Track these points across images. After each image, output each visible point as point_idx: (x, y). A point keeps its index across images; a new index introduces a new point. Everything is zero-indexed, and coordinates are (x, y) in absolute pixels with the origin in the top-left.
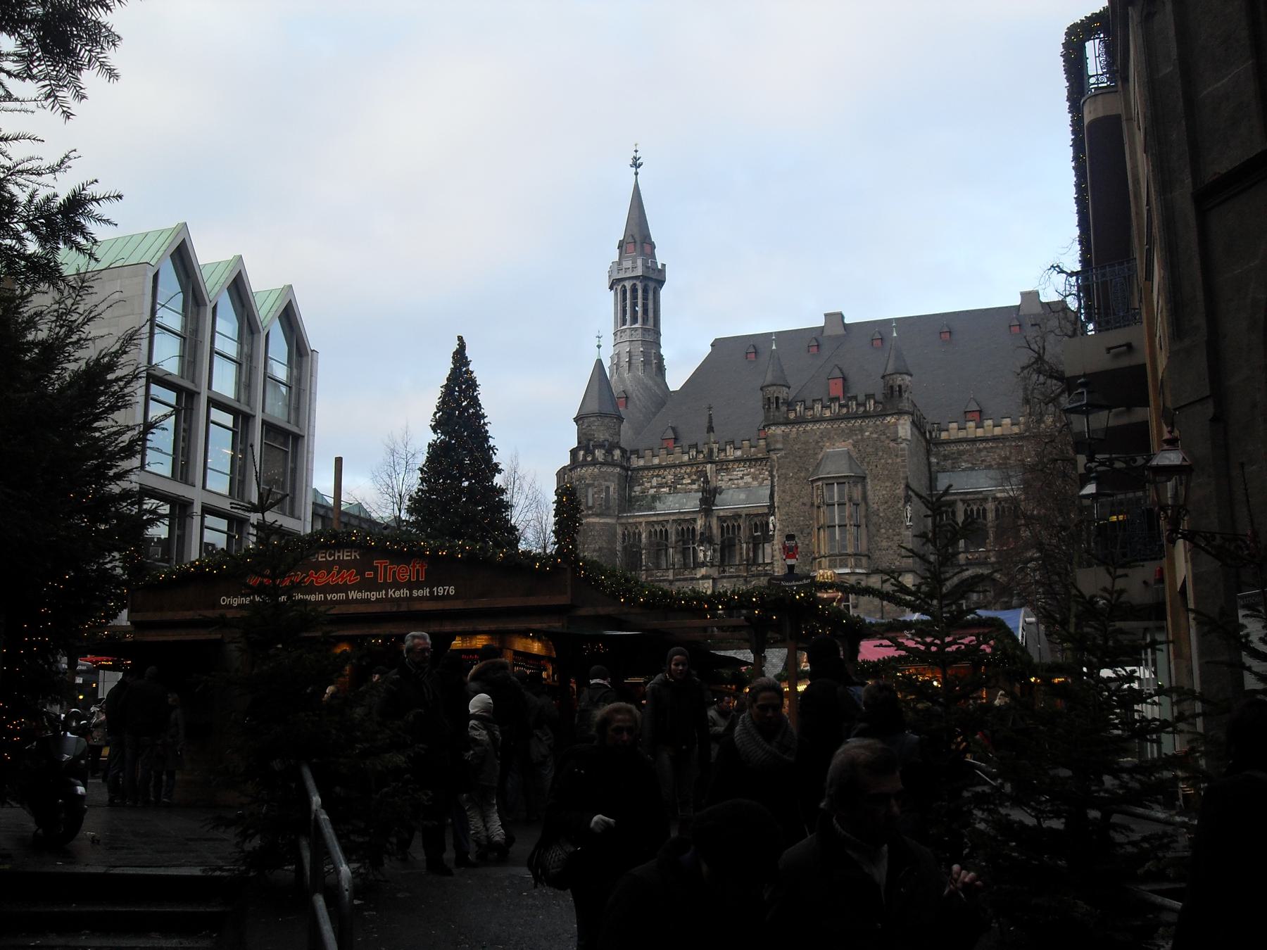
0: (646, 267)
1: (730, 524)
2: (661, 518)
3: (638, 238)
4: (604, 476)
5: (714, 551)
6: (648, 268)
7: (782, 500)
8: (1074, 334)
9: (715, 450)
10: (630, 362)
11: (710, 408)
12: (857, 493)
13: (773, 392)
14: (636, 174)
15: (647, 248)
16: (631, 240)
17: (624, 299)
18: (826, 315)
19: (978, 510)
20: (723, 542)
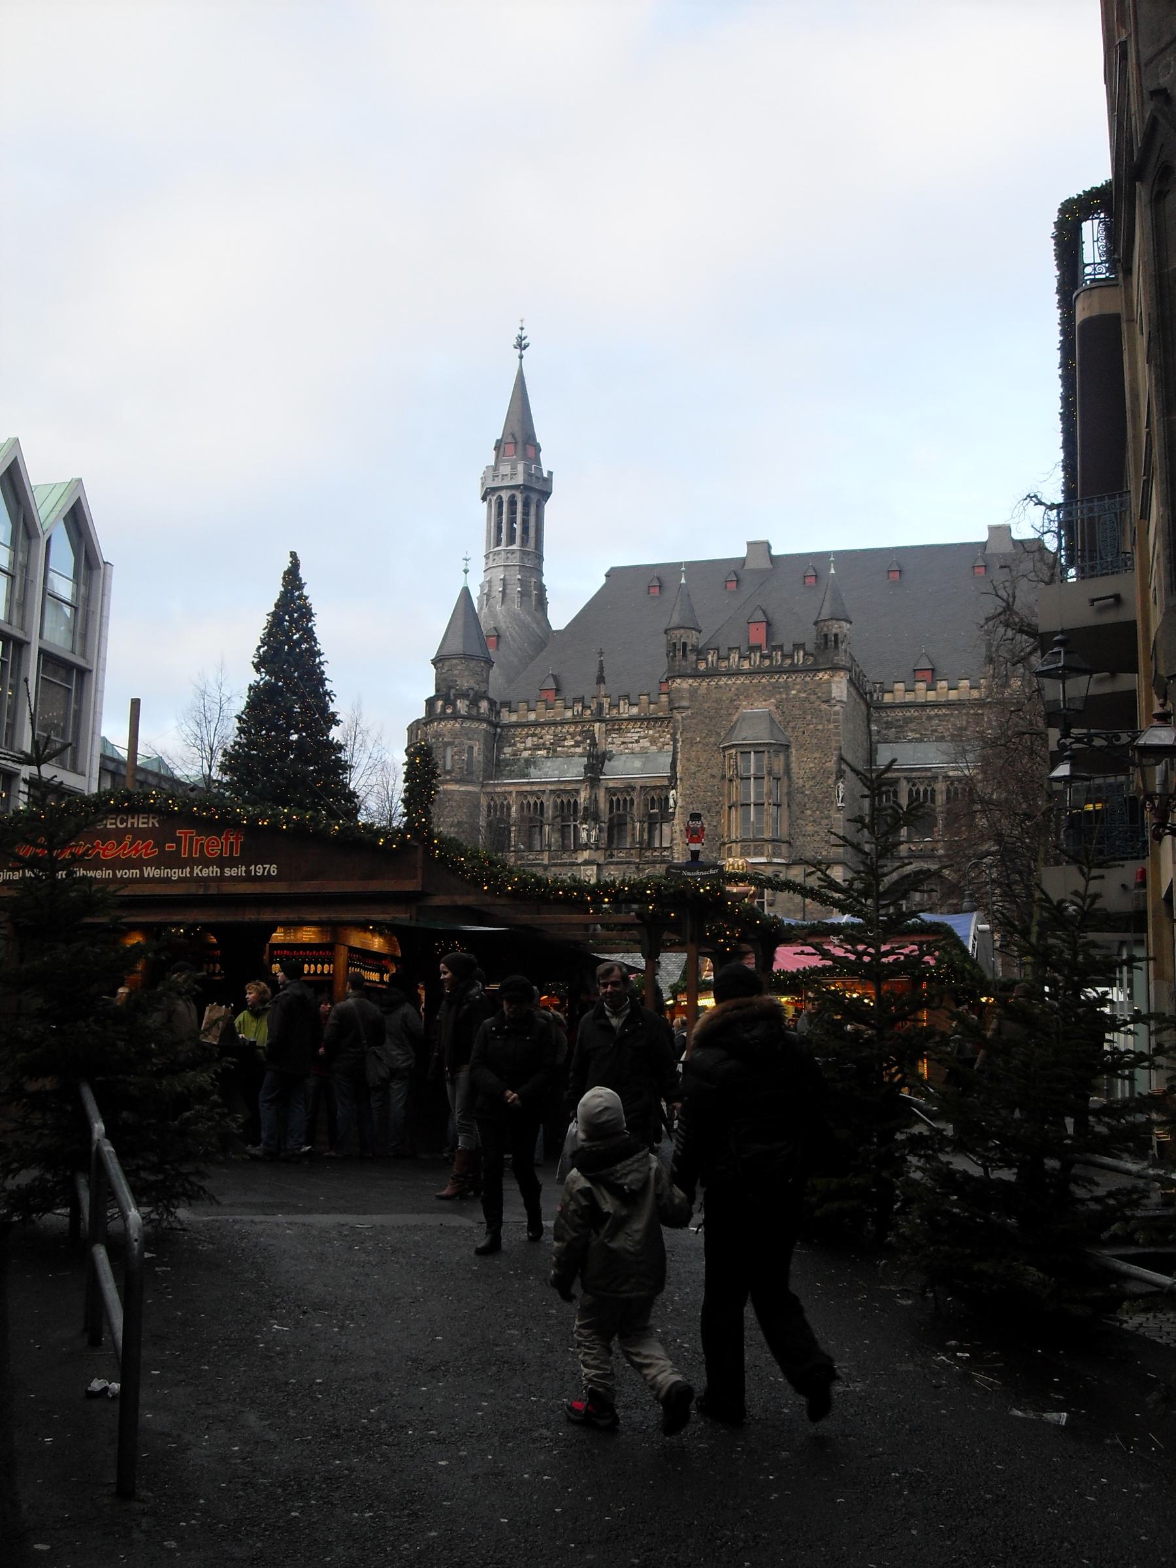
0: (528, 474)
1: (621, 798)
2: (536, 788)
3: (520, 438)
4: (467, 734)
5: (601, 830)
6: (530, 475)
7: (686, 769)
8: (1050, 582)
9: (606, 706)
10: (504, 592)
11: (601, 654)
12: (778, 765)
13: (680, 636)
14: (521, 357)
15: (531, 451)
16: (510, 439)
17: (500, 514)
18: (749, 544)
19: (926, 791)
20: (611, 820)
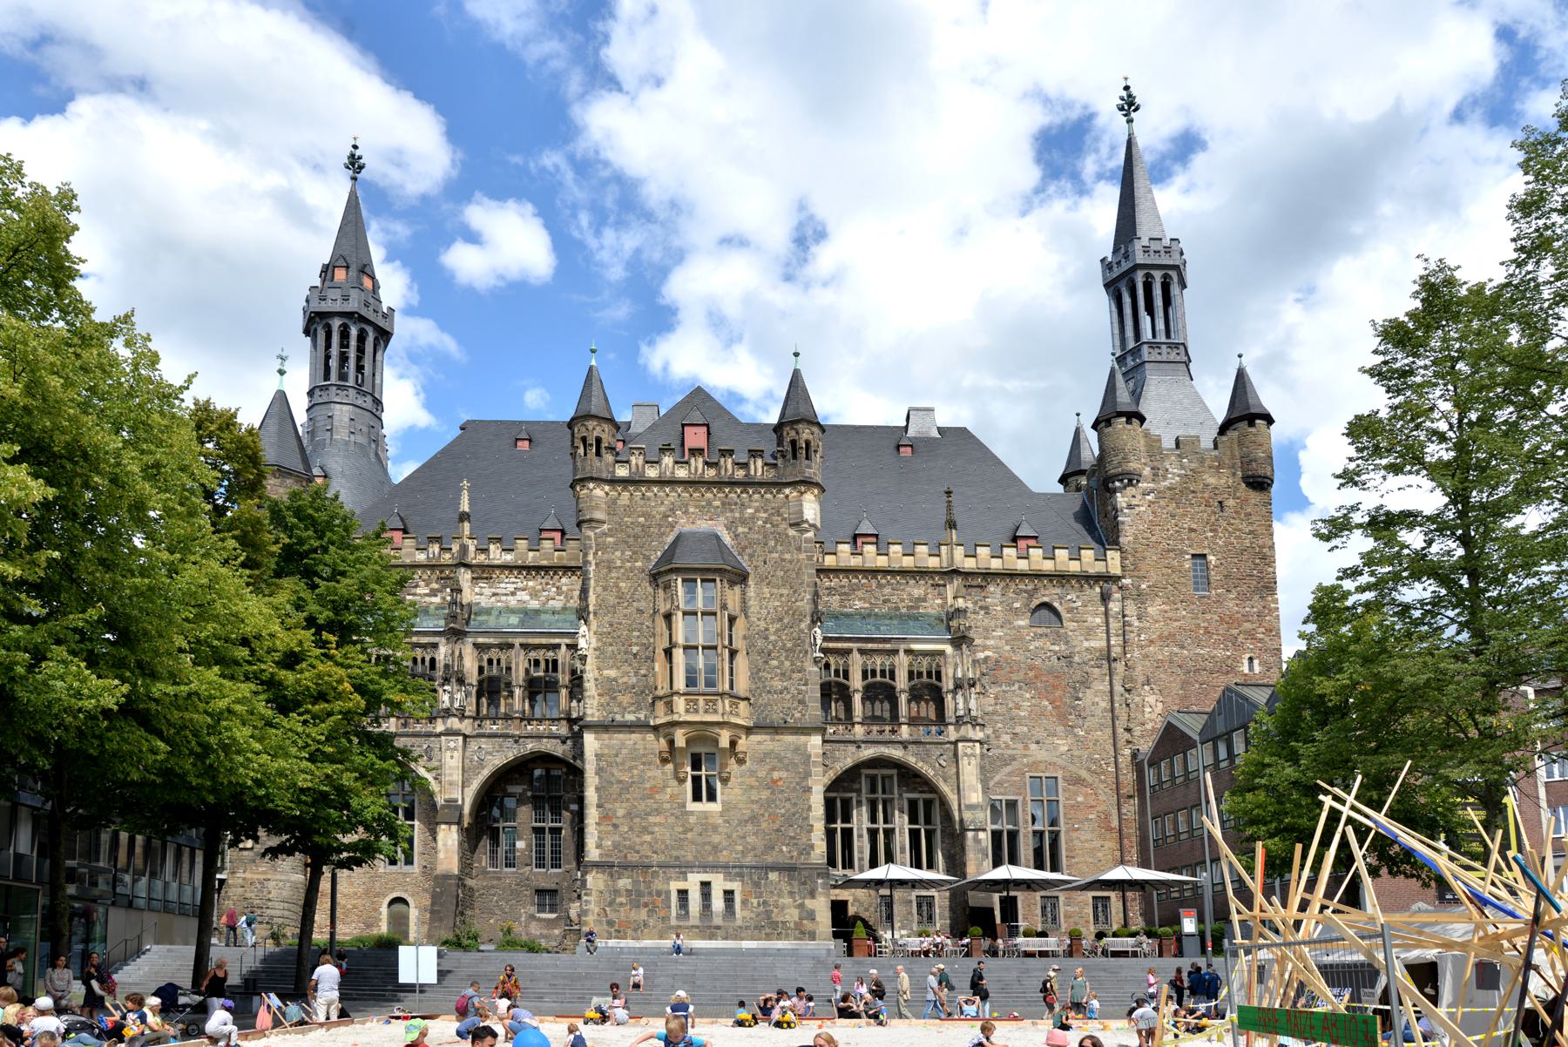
9: (472, 549)
